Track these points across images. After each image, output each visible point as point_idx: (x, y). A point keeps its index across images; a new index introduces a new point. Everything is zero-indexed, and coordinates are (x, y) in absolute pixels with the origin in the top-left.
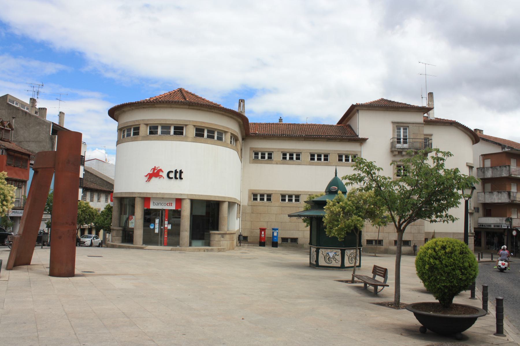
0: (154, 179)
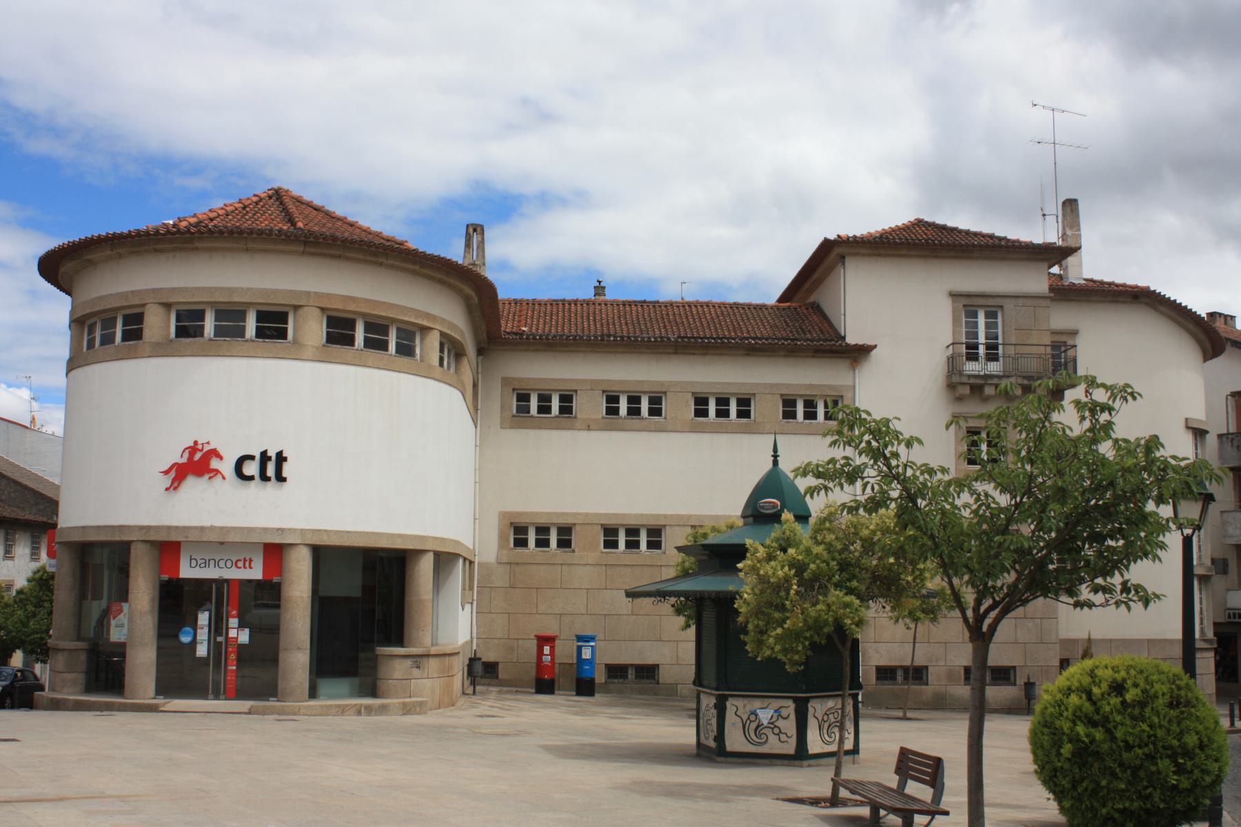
0: (191, 482)
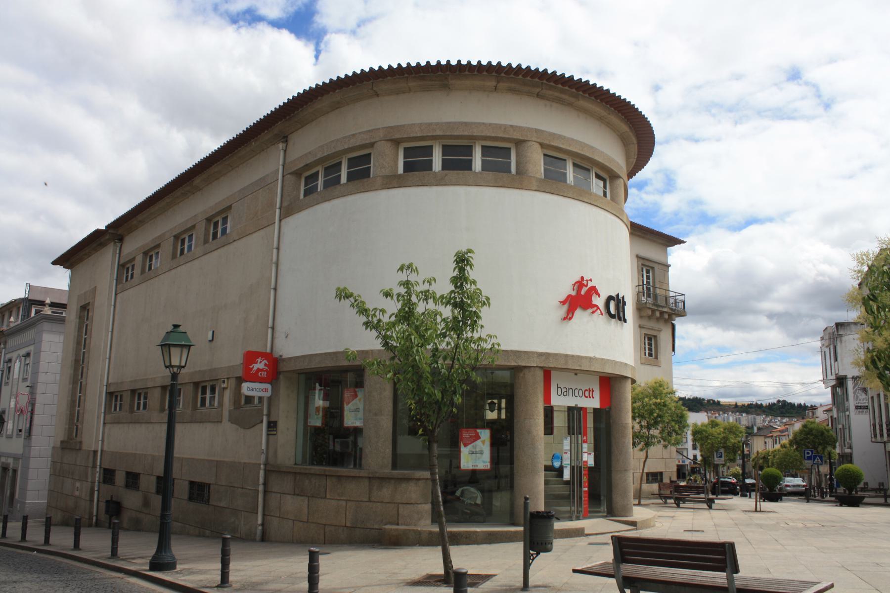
0: (580, 315)
